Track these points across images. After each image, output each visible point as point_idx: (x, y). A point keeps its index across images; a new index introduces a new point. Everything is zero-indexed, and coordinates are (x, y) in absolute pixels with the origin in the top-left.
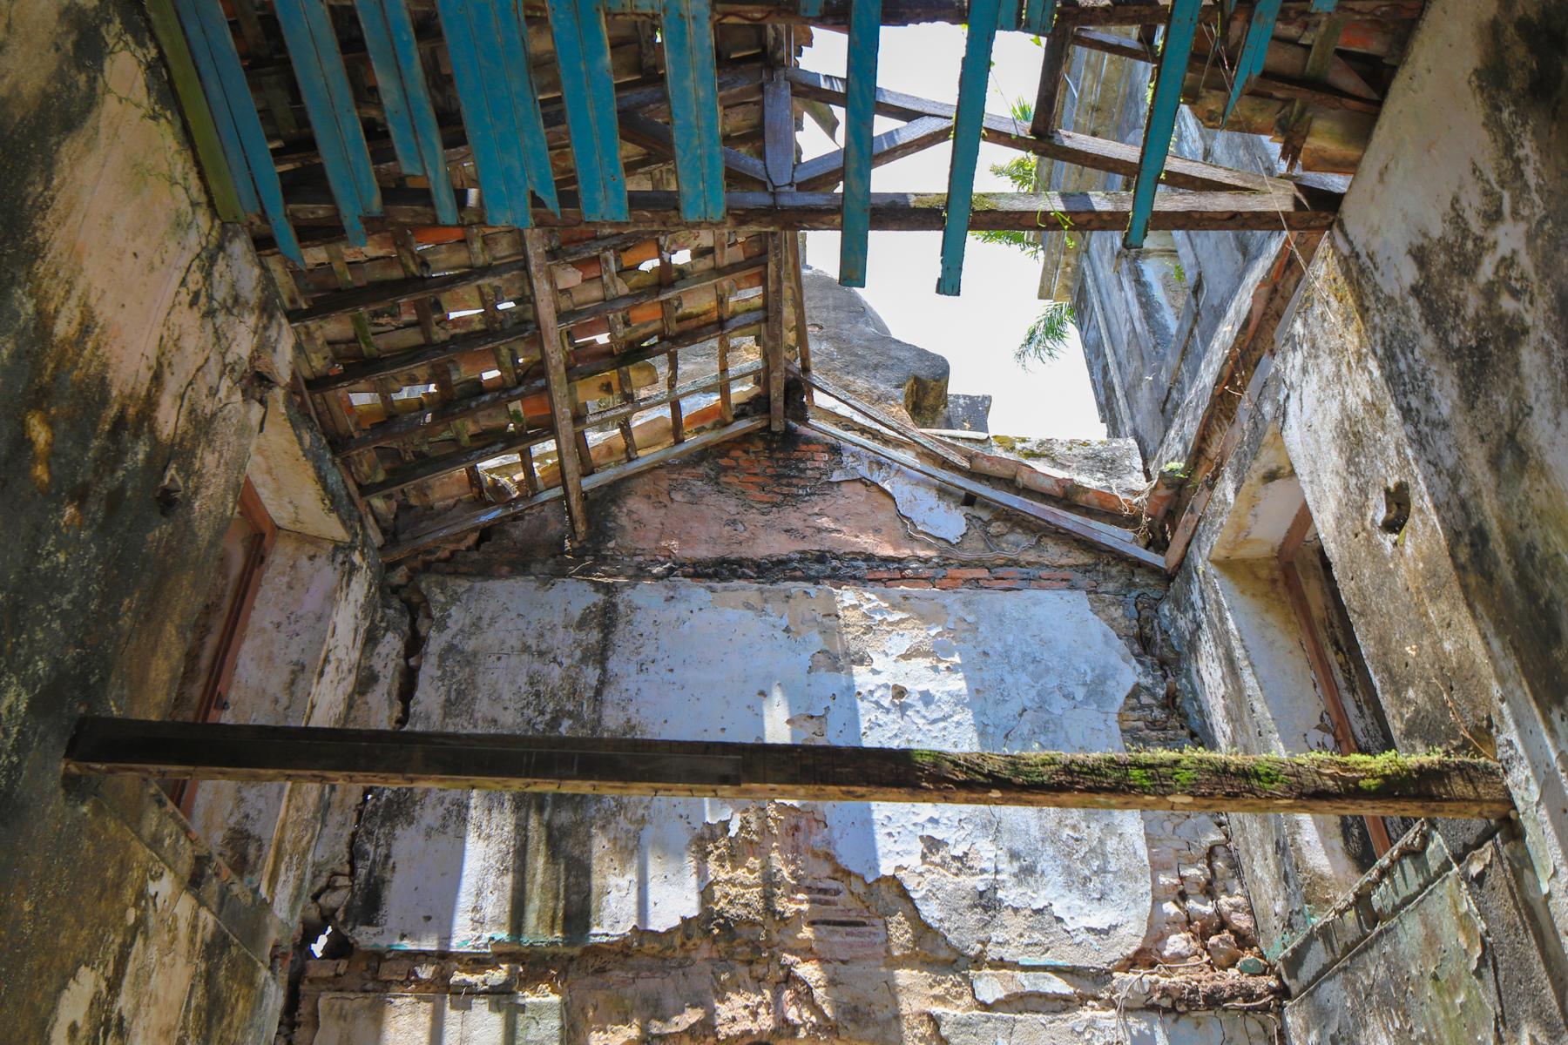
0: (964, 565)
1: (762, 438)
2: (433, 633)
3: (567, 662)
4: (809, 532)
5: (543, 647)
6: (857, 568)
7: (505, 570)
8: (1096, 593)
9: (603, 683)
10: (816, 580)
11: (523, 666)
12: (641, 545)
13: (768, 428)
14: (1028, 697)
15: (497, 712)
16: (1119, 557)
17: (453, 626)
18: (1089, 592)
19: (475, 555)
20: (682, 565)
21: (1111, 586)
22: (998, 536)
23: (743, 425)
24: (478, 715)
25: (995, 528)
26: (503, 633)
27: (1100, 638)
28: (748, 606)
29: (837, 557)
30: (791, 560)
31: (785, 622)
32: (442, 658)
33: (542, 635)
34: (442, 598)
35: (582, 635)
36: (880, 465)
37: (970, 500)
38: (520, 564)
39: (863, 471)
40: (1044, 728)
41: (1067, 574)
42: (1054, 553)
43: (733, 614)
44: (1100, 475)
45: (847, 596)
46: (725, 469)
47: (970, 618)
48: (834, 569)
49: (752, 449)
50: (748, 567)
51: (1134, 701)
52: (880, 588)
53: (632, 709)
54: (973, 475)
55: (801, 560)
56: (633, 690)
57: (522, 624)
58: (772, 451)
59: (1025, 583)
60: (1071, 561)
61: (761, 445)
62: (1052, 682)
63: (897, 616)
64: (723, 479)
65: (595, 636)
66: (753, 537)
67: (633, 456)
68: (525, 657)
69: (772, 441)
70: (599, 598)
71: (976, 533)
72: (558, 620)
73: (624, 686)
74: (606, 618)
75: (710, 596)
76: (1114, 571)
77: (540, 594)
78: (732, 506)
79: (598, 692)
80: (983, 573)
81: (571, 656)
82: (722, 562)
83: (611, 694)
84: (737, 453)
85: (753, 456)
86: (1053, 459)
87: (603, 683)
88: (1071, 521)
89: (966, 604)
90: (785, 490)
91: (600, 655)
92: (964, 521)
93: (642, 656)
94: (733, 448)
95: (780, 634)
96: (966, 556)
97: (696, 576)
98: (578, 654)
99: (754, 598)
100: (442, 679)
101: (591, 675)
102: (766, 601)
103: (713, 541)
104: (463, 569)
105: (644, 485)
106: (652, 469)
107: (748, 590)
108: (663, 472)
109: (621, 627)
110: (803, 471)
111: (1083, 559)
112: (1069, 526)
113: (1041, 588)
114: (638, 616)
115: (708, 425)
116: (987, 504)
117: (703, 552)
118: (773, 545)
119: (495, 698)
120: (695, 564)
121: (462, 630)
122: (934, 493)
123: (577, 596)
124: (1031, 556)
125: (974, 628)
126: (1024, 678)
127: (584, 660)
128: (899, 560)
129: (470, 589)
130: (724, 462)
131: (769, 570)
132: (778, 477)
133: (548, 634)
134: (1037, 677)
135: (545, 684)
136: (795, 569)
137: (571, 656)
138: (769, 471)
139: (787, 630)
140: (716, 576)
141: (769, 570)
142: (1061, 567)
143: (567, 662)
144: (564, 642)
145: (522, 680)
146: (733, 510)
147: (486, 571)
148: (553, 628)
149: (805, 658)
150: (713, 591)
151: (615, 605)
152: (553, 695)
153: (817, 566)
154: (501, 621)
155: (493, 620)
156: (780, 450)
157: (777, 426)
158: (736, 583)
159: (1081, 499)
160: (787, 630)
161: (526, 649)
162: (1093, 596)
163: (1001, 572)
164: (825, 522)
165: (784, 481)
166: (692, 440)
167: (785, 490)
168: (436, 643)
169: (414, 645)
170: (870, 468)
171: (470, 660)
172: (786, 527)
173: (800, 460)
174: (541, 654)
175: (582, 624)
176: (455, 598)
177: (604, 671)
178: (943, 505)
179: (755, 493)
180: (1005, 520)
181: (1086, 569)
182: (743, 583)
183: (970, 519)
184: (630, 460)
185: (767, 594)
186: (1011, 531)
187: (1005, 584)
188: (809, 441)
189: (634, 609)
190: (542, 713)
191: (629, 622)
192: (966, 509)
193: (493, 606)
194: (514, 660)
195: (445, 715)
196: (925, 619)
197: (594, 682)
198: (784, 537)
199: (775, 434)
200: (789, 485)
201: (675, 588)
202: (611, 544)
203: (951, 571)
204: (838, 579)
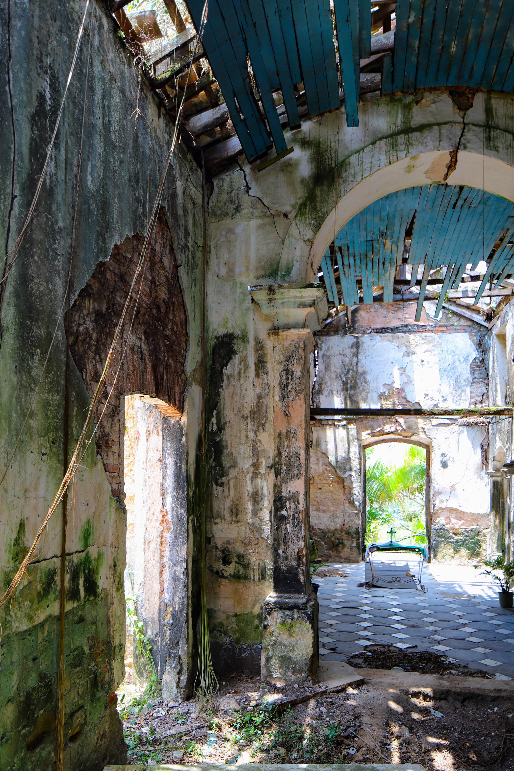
0: (441, 326)
9: (358, 362)
10: (405, 332)
14: (450, 361)
15: (336, 370)
21: (475, 331)
27: (469, 345)
28: (389, 341)
31: (397, 344)
32: (323, 357)
38: (336, 332)
40: (453, 369)
42: (463, 322)
43: (385, 343)
45: (412, 337)
52: (420, 334)
57: (338, 348)
62: (456, 357)
63: (423, 341)
65: (355, 350)
70: (355, 340)
71: (444, 317)
72: (346, 346)
74: (357, 345)
75: (380, 338)
79: (357, 364)
80: (444, 329)
83: (359, 364)
87: (358, 362)
88: (468, 313)
89: (440, 338)
91: (356, 355)
95: (396, 348)
96: (442, 324)
99: (391, 338)
107: (388, 335)
111: (470, 323)
112: (467, 316)
114: (364, 344)
119: (335, 367)
123: (349, 339)
125: (441, 344)
126: (450, 357)
127: (353, 356)
134: (453, 356)
140: (381, 332)
144: (349, 352)
145: (340, 362)
147: (328, 334)
149: (402, 354)
150: (381, 336)
155: (332, 347)
158: (386, 334)
161: (340, 354)
163: (449, 328)
164: (407, 316)
171: (328, 357)
175: (352, 347)
176: (323, 342)
181: (470, 326)
182: (388, 334)
189: (363, 343)
193: (331, 344)
196: (429, 342)
201: (372, 336)
204: (410, 332)
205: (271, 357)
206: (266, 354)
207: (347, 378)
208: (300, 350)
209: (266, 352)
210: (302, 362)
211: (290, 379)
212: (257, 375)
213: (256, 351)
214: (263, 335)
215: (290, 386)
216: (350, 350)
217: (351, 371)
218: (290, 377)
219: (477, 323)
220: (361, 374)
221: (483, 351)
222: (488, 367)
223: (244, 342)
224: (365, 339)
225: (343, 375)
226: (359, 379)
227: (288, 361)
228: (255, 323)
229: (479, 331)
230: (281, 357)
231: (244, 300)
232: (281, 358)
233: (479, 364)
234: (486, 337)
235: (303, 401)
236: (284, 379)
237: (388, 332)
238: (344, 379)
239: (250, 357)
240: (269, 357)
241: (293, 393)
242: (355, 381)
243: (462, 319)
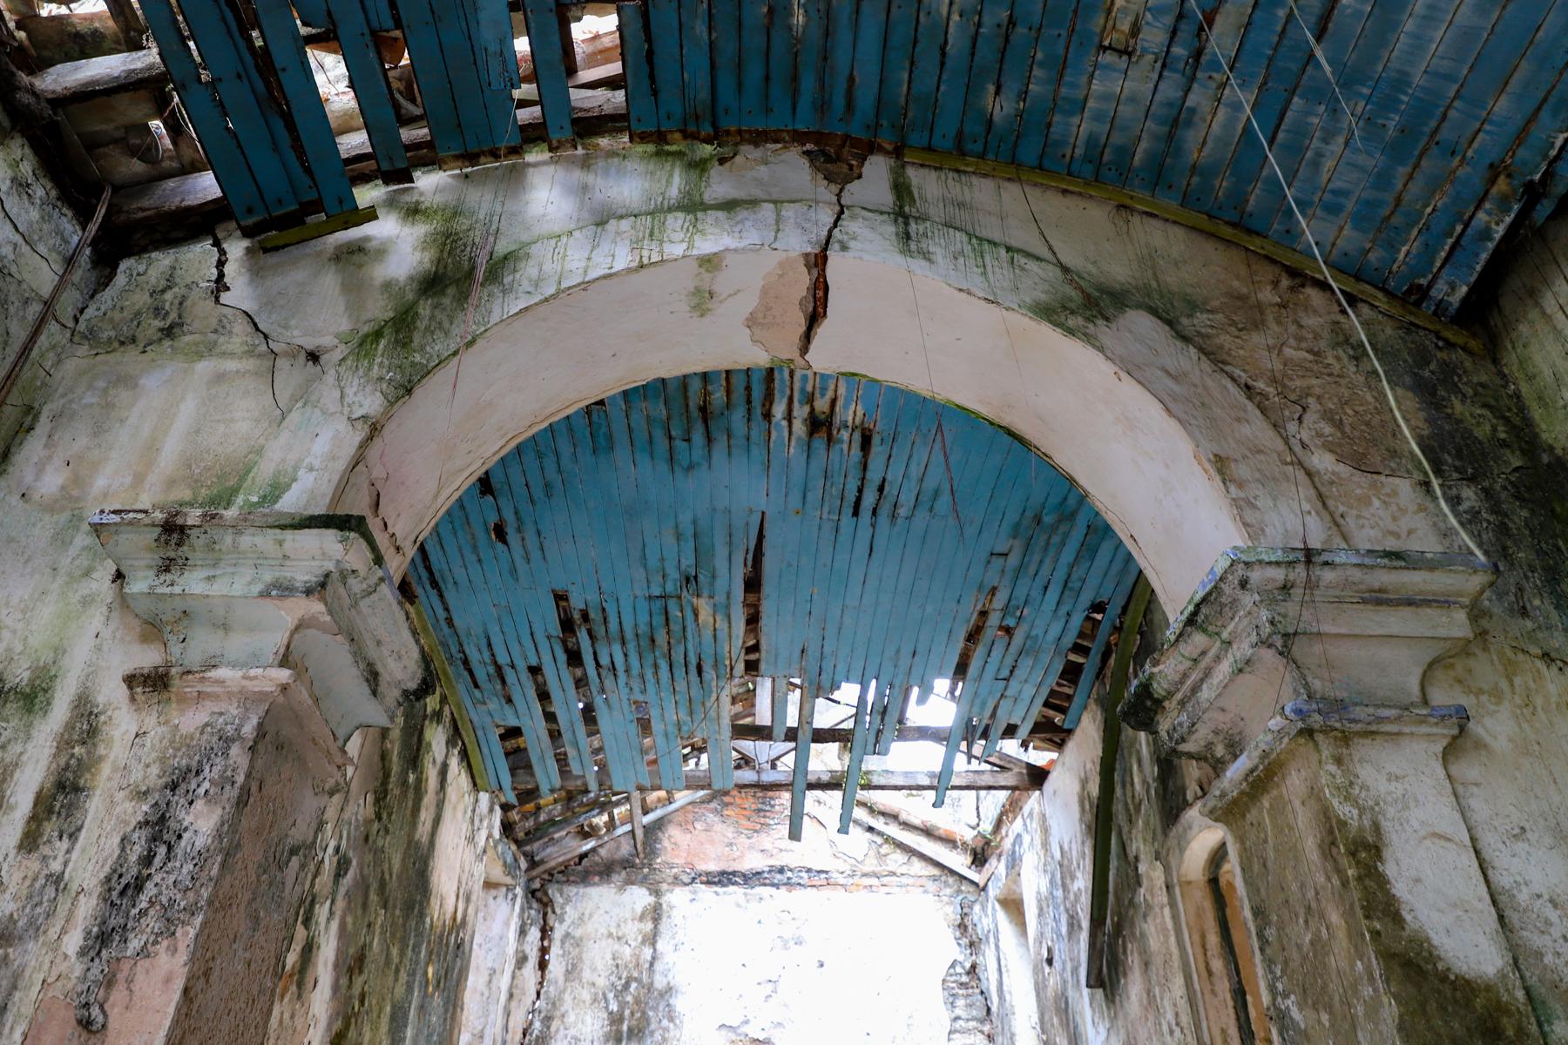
0: (865, 875)
2: (557, 925)
3: (633, 944)
4: (775, 852)
5: (620, 934)
6: (801, 878)
7: (597, 879)
9: (654, 958)
10: (777, 886)
11: (609, 947)
12: (676, 861)
17: (568, 921)
19: (579, 868)
21: (948, 891)
24: (584, 980)
25: (886, 849)
26: (597, 925)
28: (738, 905)
29: (791, 870)
32: (563, 942)
34: (561, 900)
35: (642, 926)
37: (871, 829)
42: (918, 867)
46: (727, 805)
48: (789, 878)
51: (952, 971)
53: (670, 977)
55: (770, 872)
56: (671, 965)
57: (607, 917)
60: (927, 873)
64: (725, 812)
65: (649, 926)
68: (610, 941)
70: (652, 900)
71: (872, 853)
72: (628, 915)
73: (666, 961)
74: (655, 914)
77: (617, 897)
78: (730, 833)
79: (652, 964)
80: (874, 881)
81: (636, 940)
82: (723, 873)
83: (658, 966)
90: (762, 820)
91: (652, 939)
96: (866, 869)
97: (708, 883)
98: (640, 939)
99: (742, 900)
100: (563, 956)
101: (647, 953)
103: (718, 858)
104: (572, 878)
105: (679, 817)
107: (735, 892)
109: (664, 919)
110: (773, 806)
111: (935, 871)
114: (674, 913)
116: (880, 834)
117: (713, 867)
118: (752, 862)
119: (594, 970)
120: (708, 874)
121: (573, 923)
123: (639, 897)
124: (904, 870)
127: (643, 942)
128: (827, 872)
129: (577, 894)
131: (751, 879)
132: (759, 810)
133: (622, 925)
137: (636, 940)
138: (754, 807)
140: (719, 883)
141: (751, 879)
143: (633, 944)
144: (634, 931)
145: (609, 956)
146: (730, 835)
151: (661, 905)
152: (626, 967)
153: (779, 876)
154: (596, 916)
155: (591, 915)
158: (732, 888)
159: (936, 833)
161: (610, 935)
163: (885, 880)
167: (762, 820)
168: (558, 934)
169: (545, 932)
171: (578, 943)
173: (771, 798)
174: (619, 939)
175: (642, 918)
176: (568, 900)
177: (655, 950)
179: (744, 822)
187: (886, 889)
189: (671, 907)
190: (620, 978)
191: (669, 917)
192: (868, 835)
193: (588, 906)
194: (604, 943)
195: (566, 980)
197: (649, 958)
201: (695, 892)
202: (659, 860)
203: (856, 880)
204: (789, 884)
205: (115, 770)
206: (101, 759)
207: (623, 1005)
208: (235, 750)
209: (101, 750)
210: (231, 793)
211: (157, 861)
212: (30, 841)
213: (64, 743)
214: (111, 692)
215: (150, 889)
216: (638, 925)
217: (634, 985)
218: (162, 850)
219: (952, 872)
220: (662, 995)
221: (971, 944)
222: (988, 989)
223: (30, 711)
224: (677, 898)
225: (611, 996)
226: (655, 1009)
227: (174, 787)
228: (99, 648)
229: (959, 891)
230: (155, 770)
231: (87, 573)
232: (153, 776)
233: (965, 979)
234: (977, 908)
235: (183, 956)
236: (133, 858)
237: (735, 883)
238: (614, 1007)
239: (28, 770)
240: (106, 769)
241: (152, 922)
242: (644, 1013)
243: (914, 859)
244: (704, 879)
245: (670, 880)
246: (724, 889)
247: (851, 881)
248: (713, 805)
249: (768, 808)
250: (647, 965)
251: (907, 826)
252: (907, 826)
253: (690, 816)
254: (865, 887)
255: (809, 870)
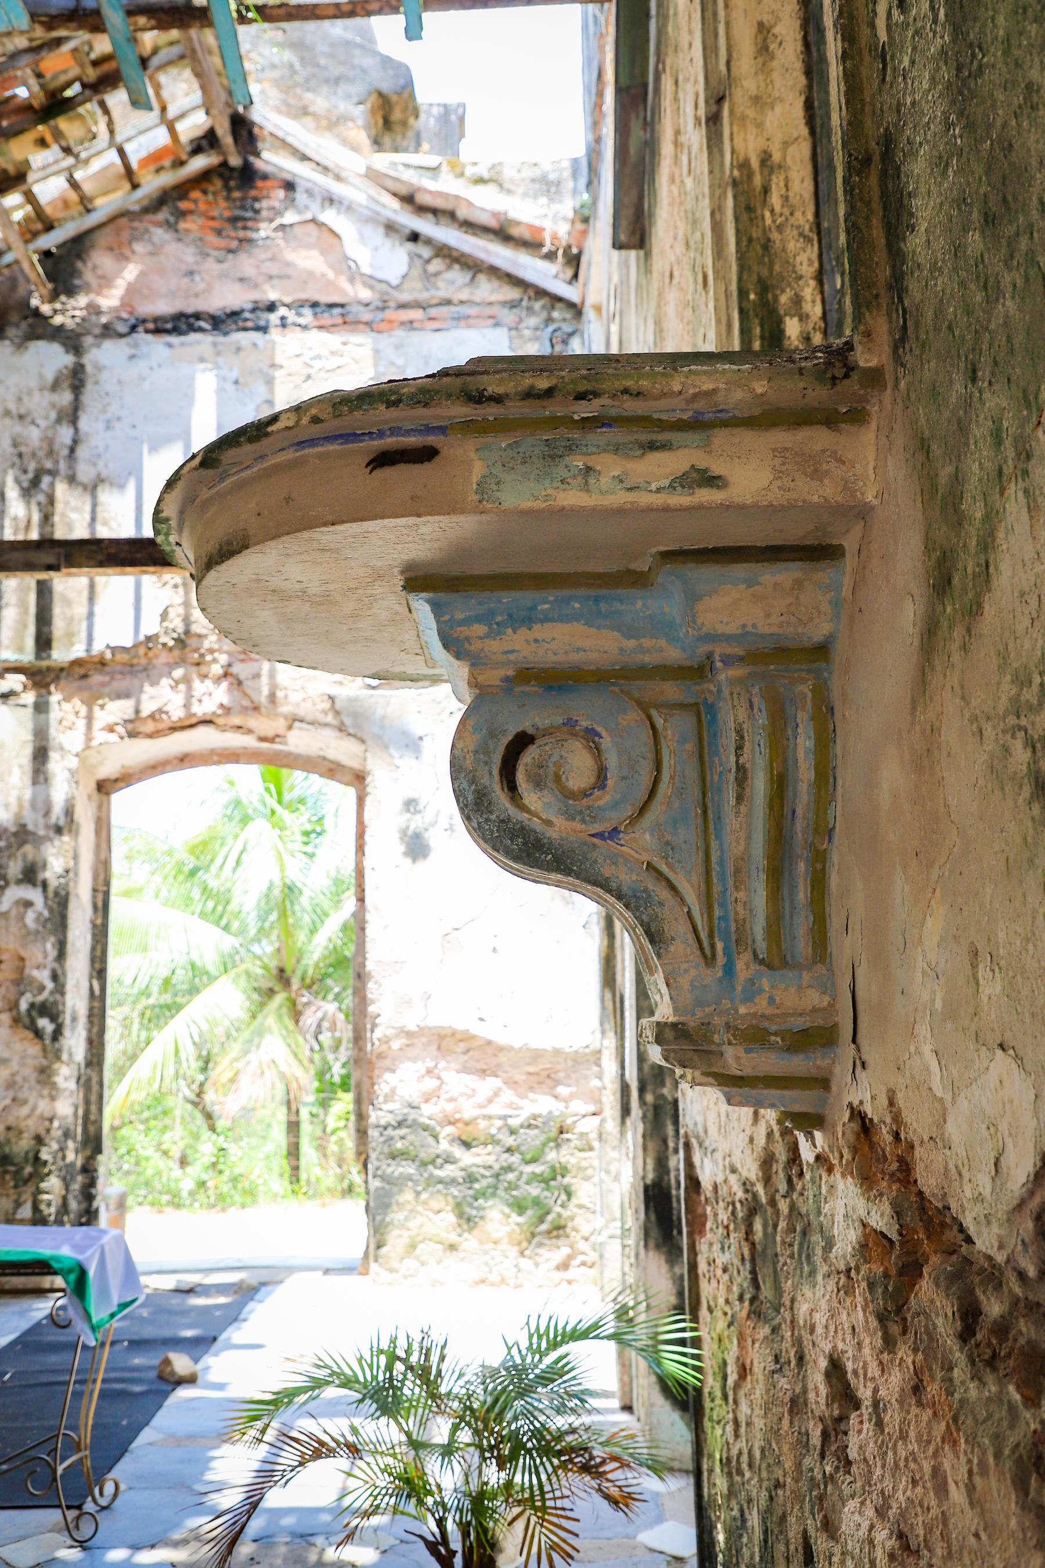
0: (402, 306)
1: (221, 176)
3: (43, 423)
5: (23, 411)
8: (517, 329)
9: (76, 441)
13: (224, 164)
16: (541, 293)
18: (510, 329)
20: (144, 321)
21: (533, 321)
22: (437, 274)
23: (199, 163)
25: (437, 265)
30: (242, 311)
31: (234, 374)
33: (19, 399)
35: (55, 398)
36: (331, 201)
37: (414, 237)
39: (314, 210)
41: (495, 310)
42: (487, 290)
44: (543, 200)
47: (399, 362)
49: (211, 188)
50: (204, 320)
53: (101, 464)
54: (422, 210)
55: (253, 310)
58: (229, 190)
59: (454, 323)
61: (218, 183)
65: (66, 397)
66: (209, 290)
67: (90, 206)
68: (7, 421)
69: (230, 178)
70: (69, 360)
71: (416, 272)
72: (33, 383)
76: (538, 305)
78: (188, 255)
79: (72, 450)
80: (417, 314)
81: (46, 418)
82: (180, 316)
83: (82, 452)
84: (196, 194)
85: (210, 197)
86: (501, 186)
87: (76, 441)
89: (398, 347)
91: (72, 415)
92: (405, 259)
93: (109, 415)
94: (193, 189)
96: (405, 297)
97: (157, 331)
98: (53, 415)
101: (65, 434)
102: (218, 354)
103: (172, 295)
105: (103, 238)
106: (113, 219)
107: (200, 342)
108: (124, 221)
111: (513, 293)
113: (469, 326)
114: (104, 376)
115: (167, 162)
116: (429, 242)
117: (164, 307)
120: (156, 320)
122: (381, 230)
124: (464, 295)
127: (59, 421)
128: (342, 306)
130: (183, 205)
133: (25, 398)
135: (27, 445)
136: (246, 320)
137: (46, 418)
138: (227, 214)
139: (236, 382)
140: (176, 331)
142: (491, 304)
143: (43, 423)
148: (30, 392)
150: (170, 345)
151: (82, 366)
152: (34, 455)
156: (239, 188)
157: (235, 161)
158: (193, 337)
159: (515, 232)
160: (236, 382)
161: (7, 413)
162: (513, 333)
163: (433, 312)
165: (240, 224)
166: (152, 183)
167: (241, 234)
170: (323, 207)
172: (240, 275)
173: (256, 199)
174: (21, 417)
175: (55, 386)
177: (76, 430)
178: (388, 243)
179: (212, 238)
180: (444, 257)
181: (513, 305)
183: (413, 256)
184: (88, 211)
185: (220, 348)
186: (449, 267)
187: (436, 325)
188: (265, 177)
189: (99, 368)
190: (25, 472)
191: (97, 383)
192: (410, 246)
198: (237, 286)
199: (232, 169)
200: (245, 228)
201: (136, 345)
203: (389, 314)
216: (49, 397)
229: (549, 320)
237: (201, 330)
243: (482, 278)
244: (151, 326)
245: (97, 331)
246: (182, 338)
247: (380, 315)
248: (163, 215)
249: (249, 214)
250: (65, 452)
251: (469, 226)
252: (469, 226)
253: (126, 235)
254: (402, 323)
255: (315, 305)
